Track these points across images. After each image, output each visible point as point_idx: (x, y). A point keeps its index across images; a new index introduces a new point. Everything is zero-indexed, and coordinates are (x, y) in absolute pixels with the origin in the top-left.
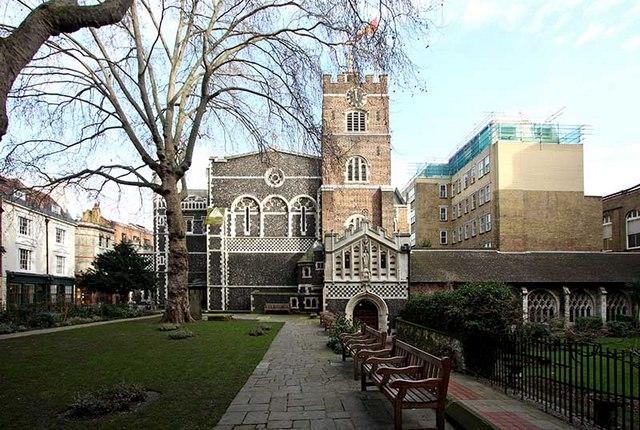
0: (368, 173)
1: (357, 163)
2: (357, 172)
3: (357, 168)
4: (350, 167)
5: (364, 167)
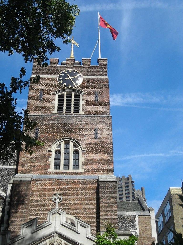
0: (82, 159)
1: (67, 149)
2: (67, 159)
3: (67, 154)
4: (58, 152)
5: (76, 152)
